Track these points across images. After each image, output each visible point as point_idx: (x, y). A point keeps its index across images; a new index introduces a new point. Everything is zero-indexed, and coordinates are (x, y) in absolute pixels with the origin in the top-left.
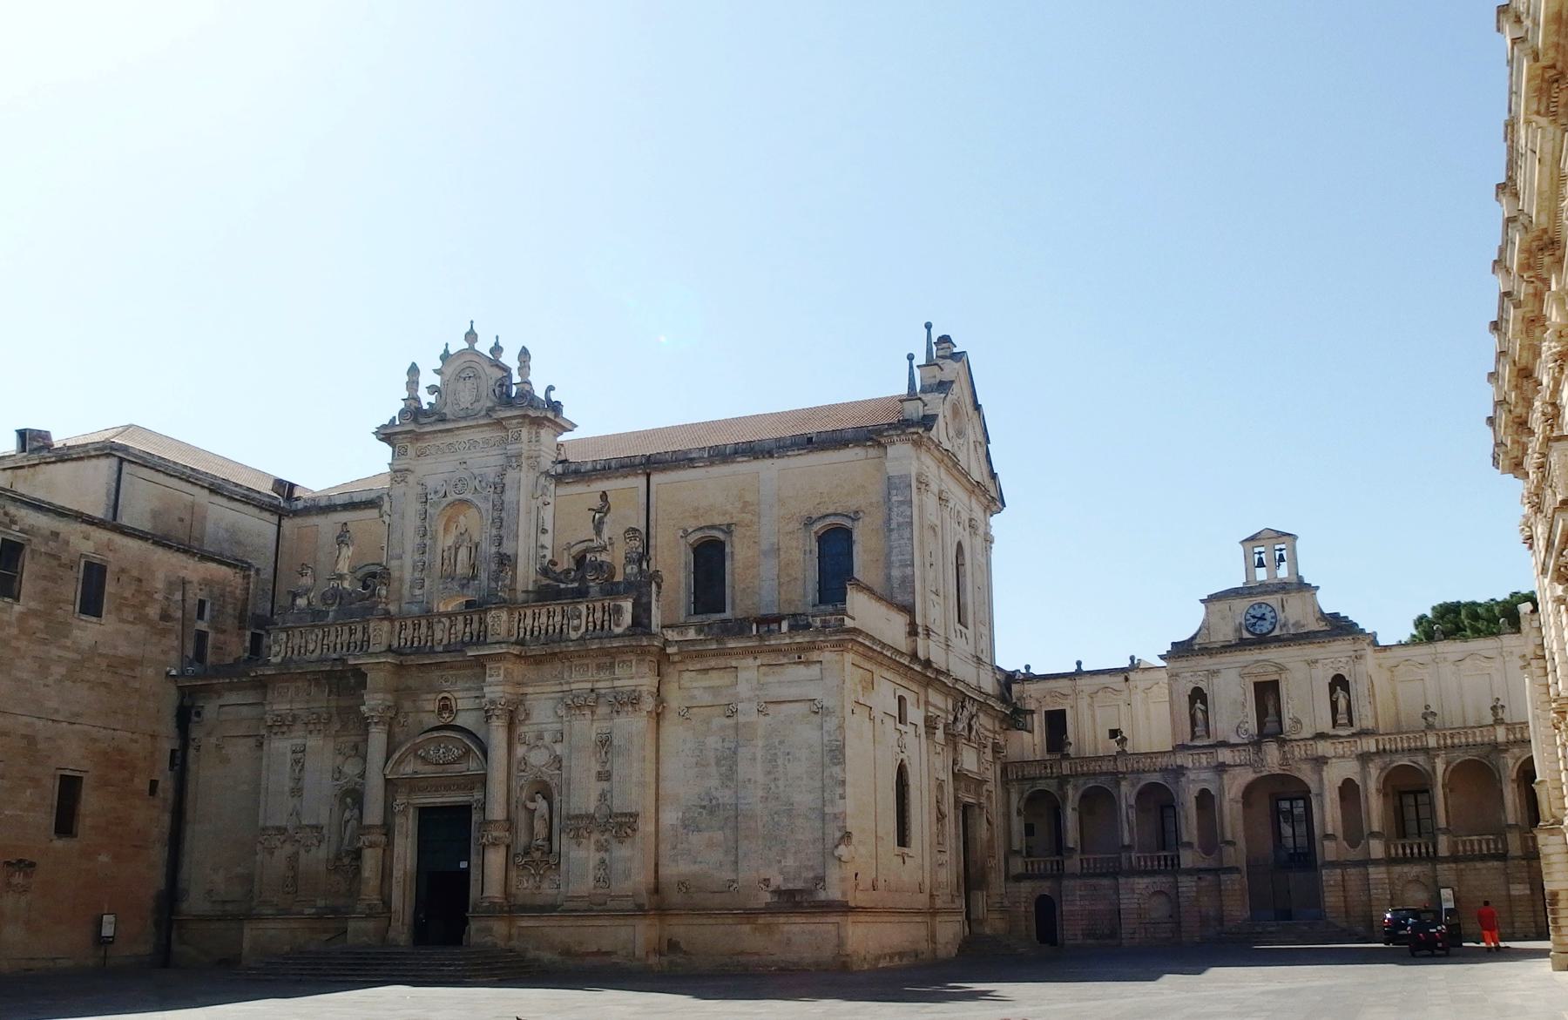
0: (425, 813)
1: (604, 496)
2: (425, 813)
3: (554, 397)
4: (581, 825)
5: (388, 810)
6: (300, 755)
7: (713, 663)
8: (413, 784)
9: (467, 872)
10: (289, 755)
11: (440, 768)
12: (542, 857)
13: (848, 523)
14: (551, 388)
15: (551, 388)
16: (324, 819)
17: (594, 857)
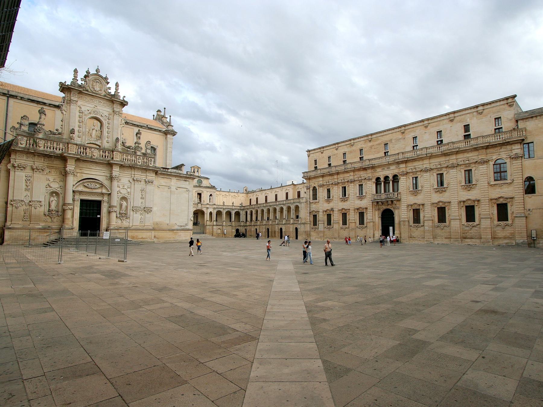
0: (82, 201)
1: (139, 130)
2: (82, 201)
3: (126, 99)
4: (135, 210)
5: (74, 200)
6: (30, 178)
7: (166, 177)
8: (81, 192)
9: (100, 218)
10: (24, 178)
11: (91, 190)
12: (123, 215)
13: (156, 148)
14: (124, 97)
15: (124, 97)
16: (42, 199)
17: (140, 217)
